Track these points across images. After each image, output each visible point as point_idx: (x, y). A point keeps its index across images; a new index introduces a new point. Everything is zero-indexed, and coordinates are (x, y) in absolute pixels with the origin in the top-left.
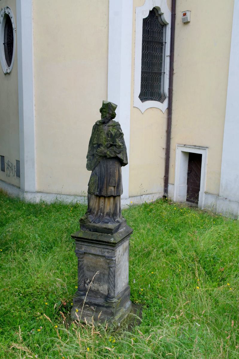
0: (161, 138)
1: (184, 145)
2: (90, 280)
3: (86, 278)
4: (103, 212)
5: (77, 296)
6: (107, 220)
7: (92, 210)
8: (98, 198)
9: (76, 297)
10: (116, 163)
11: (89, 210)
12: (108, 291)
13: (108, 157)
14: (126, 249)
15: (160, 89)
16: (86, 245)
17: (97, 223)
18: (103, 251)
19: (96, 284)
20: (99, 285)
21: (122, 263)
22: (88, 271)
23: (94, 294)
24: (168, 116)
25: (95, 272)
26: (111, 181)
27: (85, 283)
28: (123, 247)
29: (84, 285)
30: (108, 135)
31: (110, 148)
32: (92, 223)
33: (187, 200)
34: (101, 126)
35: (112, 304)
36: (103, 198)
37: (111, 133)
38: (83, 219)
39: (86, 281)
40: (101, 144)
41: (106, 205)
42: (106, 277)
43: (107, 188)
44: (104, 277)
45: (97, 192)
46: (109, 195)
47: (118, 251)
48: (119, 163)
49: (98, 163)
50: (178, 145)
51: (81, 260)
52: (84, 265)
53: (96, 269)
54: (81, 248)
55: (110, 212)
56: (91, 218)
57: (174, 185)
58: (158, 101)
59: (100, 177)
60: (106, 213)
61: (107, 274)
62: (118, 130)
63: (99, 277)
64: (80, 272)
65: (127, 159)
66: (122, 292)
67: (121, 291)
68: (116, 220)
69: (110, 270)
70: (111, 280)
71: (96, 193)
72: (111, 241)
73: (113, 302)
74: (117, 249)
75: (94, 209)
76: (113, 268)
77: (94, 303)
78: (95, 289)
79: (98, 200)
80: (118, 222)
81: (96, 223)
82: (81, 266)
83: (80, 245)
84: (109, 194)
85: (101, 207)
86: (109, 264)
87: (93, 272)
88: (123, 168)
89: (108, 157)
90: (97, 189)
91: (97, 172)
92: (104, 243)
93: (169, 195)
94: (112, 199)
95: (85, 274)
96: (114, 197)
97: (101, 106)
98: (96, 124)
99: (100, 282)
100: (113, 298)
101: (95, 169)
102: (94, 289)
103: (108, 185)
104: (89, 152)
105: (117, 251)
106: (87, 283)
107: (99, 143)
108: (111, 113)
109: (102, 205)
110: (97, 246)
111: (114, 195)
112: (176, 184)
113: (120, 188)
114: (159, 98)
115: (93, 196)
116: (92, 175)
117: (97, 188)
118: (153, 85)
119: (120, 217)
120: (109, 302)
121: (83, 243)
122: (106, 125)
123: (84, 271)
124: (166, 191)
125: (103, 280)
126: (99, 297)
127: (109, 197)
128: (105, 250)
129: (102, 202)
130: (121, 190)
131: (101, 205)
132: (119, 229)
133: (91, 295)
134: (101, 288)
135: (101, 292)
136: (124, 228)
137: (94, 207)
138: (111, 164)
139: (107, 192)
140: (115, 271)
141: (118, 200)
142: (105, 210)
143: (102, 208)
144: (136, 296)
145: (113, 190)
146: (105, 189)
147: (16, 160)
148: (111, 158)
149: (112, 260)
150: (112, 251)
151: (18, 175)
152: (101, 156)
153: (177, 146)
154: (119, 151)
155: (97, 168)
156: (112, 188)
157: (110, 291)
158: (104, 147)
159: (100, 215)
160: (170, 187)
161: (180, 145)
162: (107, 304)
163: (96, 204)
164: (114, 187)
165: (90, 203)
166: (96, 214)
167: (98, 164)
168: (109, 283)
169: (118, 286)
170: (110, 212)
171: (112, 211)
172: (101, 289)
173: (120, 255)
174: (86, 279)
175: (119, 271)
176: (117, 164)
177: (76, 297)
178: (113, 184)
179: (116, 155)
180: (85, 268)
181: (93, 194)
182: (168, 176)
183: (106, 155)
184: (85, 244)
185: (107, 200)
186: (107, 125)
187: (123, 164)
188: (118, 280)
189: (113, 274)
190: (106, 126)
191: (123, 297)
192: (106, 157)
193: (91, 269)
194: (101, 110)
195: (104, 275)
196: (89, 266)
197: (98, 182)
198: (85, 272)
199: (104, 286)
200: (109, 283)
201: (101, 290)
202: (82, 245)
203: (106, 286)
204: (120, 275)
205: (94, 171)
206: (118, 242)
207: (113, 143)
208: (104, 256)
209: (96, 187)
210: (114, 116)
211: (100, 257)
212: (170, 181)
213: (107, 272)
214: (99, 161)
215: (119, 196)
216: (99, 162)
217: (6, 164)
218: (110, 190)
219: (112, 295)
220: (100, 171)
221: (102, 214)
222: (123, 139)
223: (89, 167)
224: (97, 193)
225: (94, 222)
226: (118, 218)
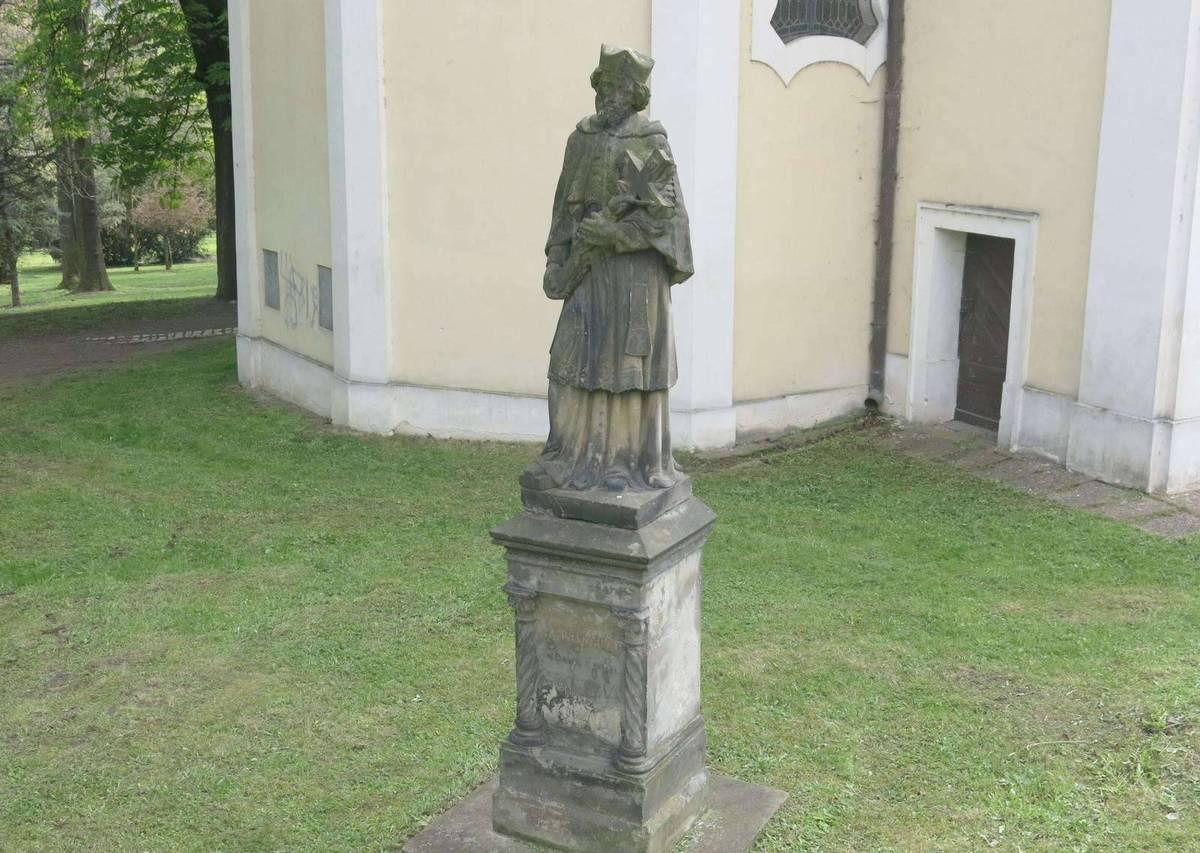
0: (860, 178)
2: (558, 692)
3: (545, 684)
4: (604, 449)
5: (511, 747)
6: (619, 477)
7: (565, 443)
8: (586, 397)
9: (511, 751)
10: (650, 270)
11: (554, 442)
12: (623, 732)
13: (620, 248)
14: (689, 584)
16: (543, 567)
17: (582, 489)
18: (602, 587)
19: (582, 706)
20: (591, 709)
21: (672, 634)
24: (887, 93)
26: (630, 337)
27: (541, 700)
29: (539, 710)
30: (620, 170)
31: (628, 218)
32: (565, 486)
33: (958, 416)
34: (596, 137)
35: (636, 776)
36: (605, 398)
37: (630, 160)
38: (533, 471)
39: (546, 693)
40: (595, 203)
41: (613, 425)
42: (615, 680)
43: (616, 363)
44: (608, 682)
46: (626, 388)
47: (657, 590)
48: (661, 272)
49: (585, 271)
50: (925, 205)
51: (525, 619)
52: (536, 636)
54: (526, 576)
55: (630, 450)
56: (559, 470)
58: (847, 37)
59: (593, 321)
60: (614, 454)
61: (618, 671)
62: (656, 153)
65: (689, 258)
66: (673, 735)
67: (672, 731)
68: (651, 479)
69: (628, 656)
70: (633, 692)
71: (577, 379)
73: (641, 768)
74: (655, 580)
75: (574, 437)
76: (639, 649)
77: (573, 771)
78: (577, 721)
79: (585, 406)
80: (658, 485)
81: (577, 489)
82: (528, 639)
83: (523, 568)
84: (625, 384)
85: (595, 432)
86: (624, 636)
87: (570, 662)
88: (676, 288)
89: (620, 248)
91: (583, 303)
92: (607, 561)
93: (887, 394)
94: (636, 404)
95: (541, 671)
96: (645, 395)
97: (594, 64)
98: (579, 129)
99: (595, 697)
100: (638, 756)
101: (576, 292)
102: (574, 724)
104: (554, 232)
105: (654, 590)
106: (548, 701)
107: (590, 198)
109: (601, 425)
110: (582, 571)
111: (642, 387)
113: (667, 362)
114: (855, 27)
115: (569, 389)
116: (565, 317)
117: (580, 360)
119: (665, 468)
120: (626, 772)
121: (530, 561)
122: (612, 132)
123: (537, 660)
124: (877, 380)
126: (592, 751)
127: (627, 394)
128: (609, 585)
129: (601, 413)
130: (670, 369)
131: (596, 423)
132: (663, 512)
133: (562, 744)
134: (595, 721)
135: (598, 733)
136: (683, 509)
138: (632, 272)
139: (617, 379)
140: (644, 662)
141: (657, 407)
143: (599, 434)
146: (609, 364)
147: (319, 266)
148: (632, 254)
149: (637, 621)
150: (633, 588)
151: (327, 324)
152: (593, 248)
154: (660, 228)
155: (582, 293)
156: (638, 364)
157: (628, 732)
158: (605, 216)
160: (892, 365)
161: (931, 204)
163: (578, 415)
164: (644, 358)
165: (558, 416)
166: (579, 458)
167: (584, 275)
168: (626, 702)
169: (659, 715)
170: (630, 450)
171: (636, 447)
172: (597, 723)
173: (665, 605)
174: (545, 688)
175: (663, 661)
176: (653, 276)
177: (511, 751)
179: (649, 243)
180: (541, 649)
181: (567, 383)
183: (613, 241)
184: (540, 563)
185: (617, 404)
186: (617, 134)
187: (677, 277)
188: (658, 693)
189: (638, 670)
190: (613, 136)
191: (677, 754)
192: (612, 249)
193: (563, 654)
194: (596, 81)
195: (607, 674)
197: (586, 341)
199: (608, 712)
200: (626, 702)
201: (599, 729)
202: (530, 568)
203: (617, 713)
204: (664, 675)
205: (571, 302)
206: (656, 558)
207: (638, 198)
208: (610, 608)
209: (576, 359)
210: (640, 101)
211: (592, 610)
213: (616, 664)
215: (664, 391)
216: (589, 268)
217: (282, 282)
218: (628, 371)
219: (637, 744)
220: (593, 305)
221: (600, 457)
222: (673, 184)
223: (552, 288)
224: (583, 380)
225: (571, 485)
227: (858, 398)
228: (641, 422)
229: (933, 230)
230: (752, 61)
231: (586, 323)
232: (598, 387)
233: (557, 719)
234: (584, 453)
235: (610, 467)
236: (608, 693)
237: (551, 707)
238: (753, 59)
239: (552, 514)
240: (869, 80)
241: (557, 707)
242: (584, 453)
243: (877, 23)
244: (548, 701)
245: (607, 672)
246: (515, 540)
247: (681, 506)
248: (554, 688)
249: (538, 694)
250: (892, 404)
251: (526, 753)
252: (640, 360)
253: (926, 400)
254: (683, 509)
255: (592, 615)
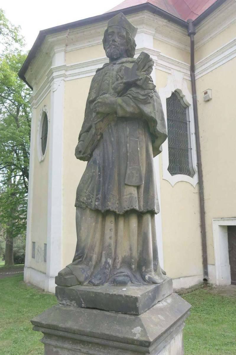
0: (195, 213)
1: (222, 218)
6: (124, 276)
7: (86, 251)
8: (100, 219)
15: (188, 165)
16: (69, 350)
24: (200, 190)
26: (128, 172)
28: (170, 352)
32: (86, 283)
33: (232, 283)
36: (113, 219)
41: (119, 238)
43: (120, 193)
45: (96, 201)
46: (127, 209)
48: (147, 134)
49: (99, 137)
50: (214, 219)
55: (131, 257)
57: (214, 265)
59: (104, 167)
60: (120, 259)
68: (147, 277)
71: (93, 204)
72: (135, 334)
75: (92, 248)
79: (99, 226)
83: (55, 350)
84: (126, 207)
85: (106, 244)
90: (97, 195)
92: (116, 344)
93: (209, 277)
94: (134, 222)
103: (122, 184)
108: (124, 34)
109: (110, 238)
112: (217, 264)
114: (190, 174)
115: (88, 211)
117: (95, 191)
118: (181, 161)
119: (155, 270)
121: (59, 344)
124: (206, 273)
131: (107, 237)
132: (156, 301)
136: (169, 300)
137: (89, 241)
138: (128, 133)
139: (120, 203)
142: (119, 251)
143: (110, 245)
145: (136, 195)
146: (115, 192)
151: (45, 261)
153: (213, 221)
155: (97, 153)
156: (134, 191)
159: (106, 262)
160: (210, 268)
161: (216, 219)
163: (95, 231)
164: (138, 187)
165: (81, 231)
166: (96, 263)
170: (131, 257)
171: (135, 254)
178: (134, 180)
179: (139, 108)
181: (87, 207)
182: (207, 256)
184: (67, 345)
202: (59, 350)
206: (156, 340)
209: (93, 190)
212: (210, 261)
214: (100, 131)
216: (102, 135)
217: (36, 250)
218: (128, 196)
221: (110, 261)
224: (97, 203)
226: (150, 271)
227: (201, 278)
228: (138, 236)
229: (218, 227)
230: (163, 179)
231: (99, 168)
232: (108, 208)
234: (99, 260)
235: (118, 269)
238: (164, 179)
239: (75, 305)
240: (194, 187)
242: (99, 260)
243: (195, 172)
246: (49, 327)
247: (168, 298)
250: (211, 281)
252: (136, 189)
253: (222, 278)
254: (169, 300)
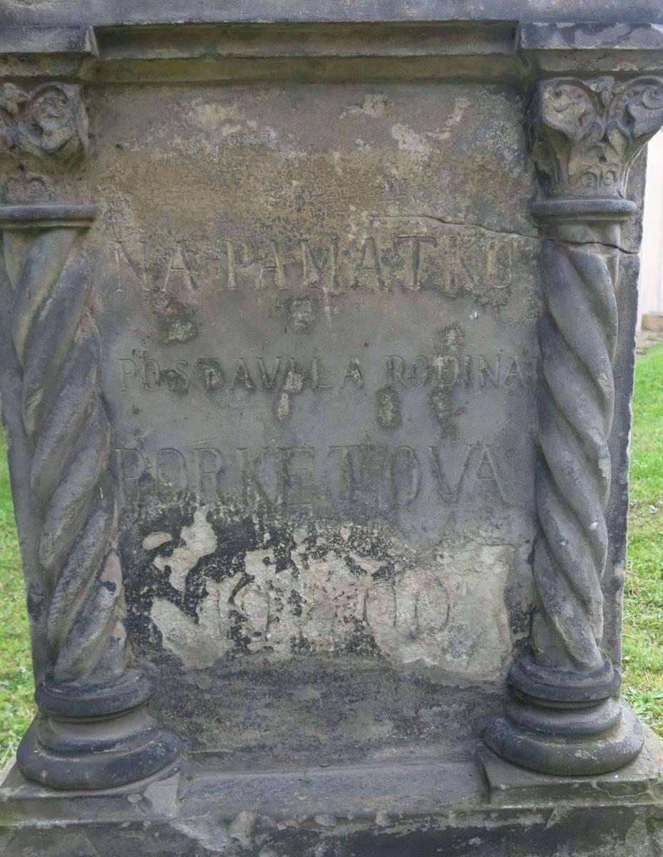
2: (219, 530)
3: (156, 508)
5: (47, 807)
9: (42, 823)
19: (333, 562)
20: (370, 565)
22: (182, 393)
23: (309, 707)
25: (294, 383)
29: (138, 627)
44: (449, 430)
53: (307, 329)
63: (368, 449)
64: (65, 419)
77: (359, 827)
78: (311, 632)
82: (60, 314)
87: (271, 385)
95: (133, 457)
99: (391, 515)
102: (301, 644)
106: (177, 581)
125: (430, 483)
126: (385, 729)
133: (251, 736)
135: (410, 655)
144: (380, 729)
162: (565, 792)
172: (405, 614)
196: (191, 298)
198: (125, 421)
199: (453, 564)
201: (412, 638)
203: (489, 555)
233: (226, 645)
236: (453, 481)
237: (189, 602)
241: (217, 596)
244: (177, 581)
245: (448, 393)
248: (200, 516)
249: (125, 561)
251: (110, 815)
255: (380, 137)
